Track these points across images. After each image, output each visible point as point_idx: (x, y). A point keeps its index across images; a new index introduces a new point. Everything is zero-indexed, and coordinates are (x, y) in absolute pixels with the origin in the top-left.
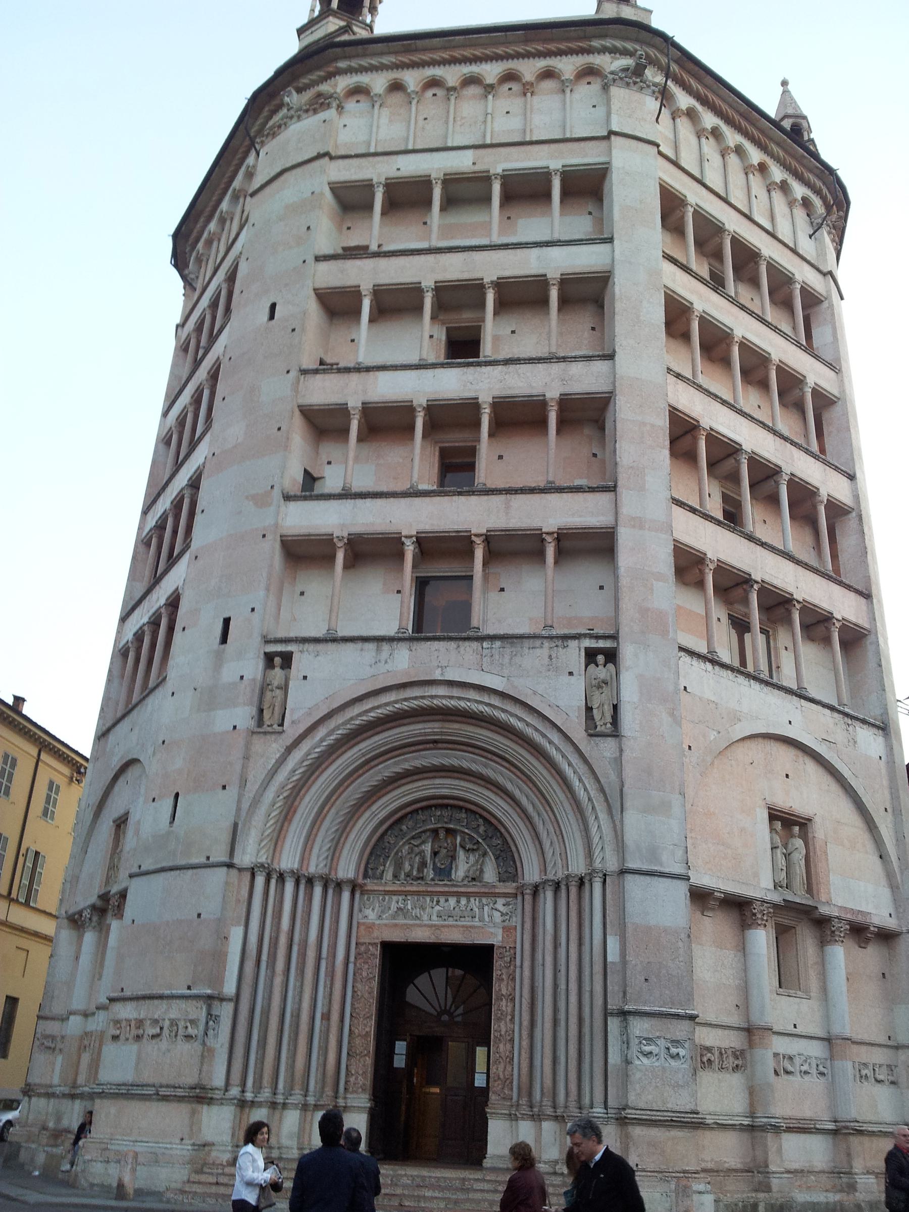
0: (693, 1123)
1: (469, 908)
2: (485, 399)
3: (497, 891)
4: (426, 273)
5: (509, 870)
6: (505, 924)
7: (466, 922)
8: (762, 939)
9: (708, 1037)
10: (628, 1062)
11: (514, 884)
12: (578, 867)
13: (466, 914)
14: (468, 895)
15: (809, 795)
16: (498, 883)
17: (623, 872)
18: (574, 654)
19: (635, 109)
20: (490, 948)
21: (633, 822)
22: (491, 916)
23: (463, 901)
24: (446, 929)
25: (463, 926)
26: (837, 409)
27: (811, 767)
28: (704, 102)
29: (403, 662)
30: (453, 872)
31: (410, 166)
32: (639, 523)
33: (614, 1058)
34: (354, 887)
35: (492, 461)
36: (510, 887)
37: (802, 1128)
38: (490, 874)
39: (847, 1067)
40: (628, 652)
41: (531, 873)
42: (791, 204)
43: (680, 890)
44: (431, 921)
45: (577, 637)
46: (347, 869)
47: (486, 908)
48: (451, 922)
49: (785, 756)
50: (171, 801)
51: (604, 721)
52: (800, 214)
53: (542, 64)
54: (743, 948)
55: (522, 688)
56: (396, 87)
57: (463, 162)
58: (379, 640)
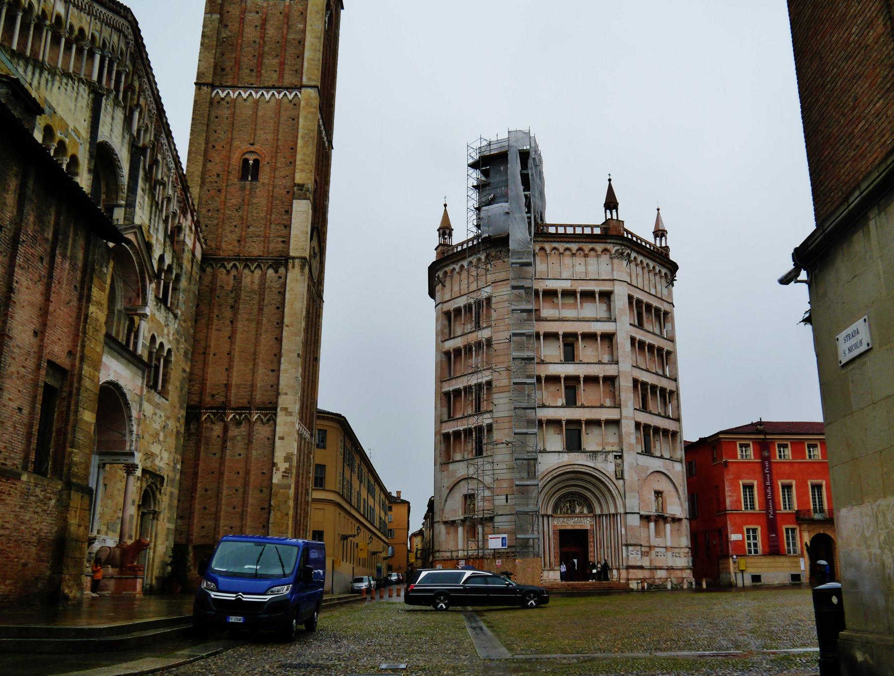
0: (641, 568)
2: (582, 376)
4: (561, 328)
8: (652, 525)
9: (643, 549)
10: (628, 556)
12: (612, 511)
15: (663, 485)
17: (626, 513)
18: (611, 457)
19: (621, 269)
20: (585, 532)
21: (628, 502)
26: (672, 356)
27: (664, 477)
28: (638, 253)
29: (567, 458)
31: (551, 285)
32: (626, 418)
33: (624, 555)
34: (552, 516)
35: (585, 394)
36: (591, 515)
37: (661, 568)
38: (585, 511)
39: (669, 554)
40: (625, 455)
41: (598, 512)
42: (661, 277)
43: (638, 516)
44: (571, 524)
45: (613, 451)
46: (550, 512)
49: (655, 474)
50: (504, 497)
51: (620, 476)
52: (663, 280)
53: (591, 246)
54: (648, 527)
55: (599, 466)
56: (542, 249)
57: (567, 285)
58: (559, 452)
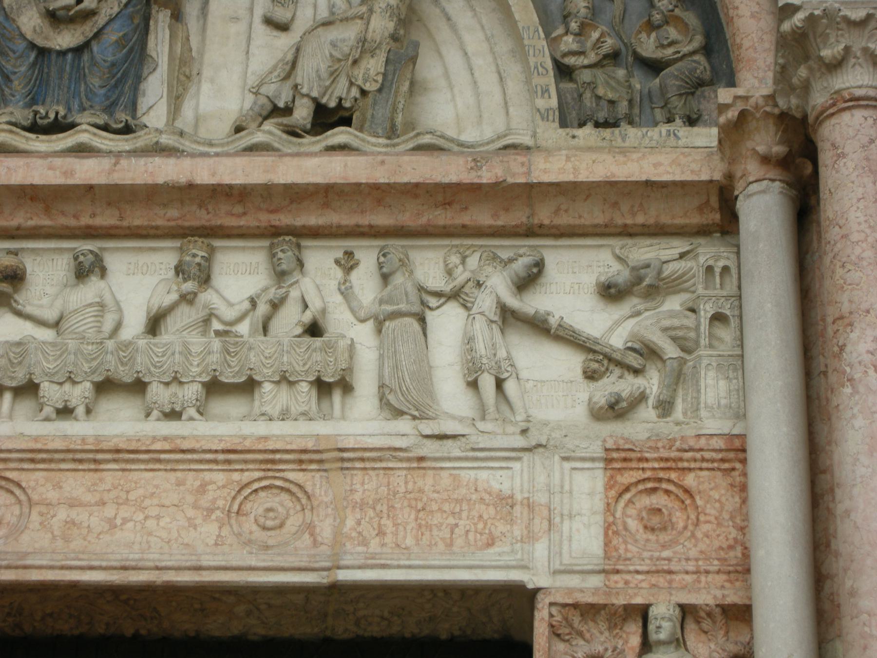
1: (290, 320)
3: (550, 169)
5: (648, 46)
6: (642, 427)
7: (277, 421)
11: (706, 136)
13: (261, 355)
14: (282, 221)
16: (551, 134)
22: (488, 381)
23: (240, 276)
24: (75, 484)
25: (230, 456)
30: (154, 89)
47: (447, 323)
48: (120, 422)
